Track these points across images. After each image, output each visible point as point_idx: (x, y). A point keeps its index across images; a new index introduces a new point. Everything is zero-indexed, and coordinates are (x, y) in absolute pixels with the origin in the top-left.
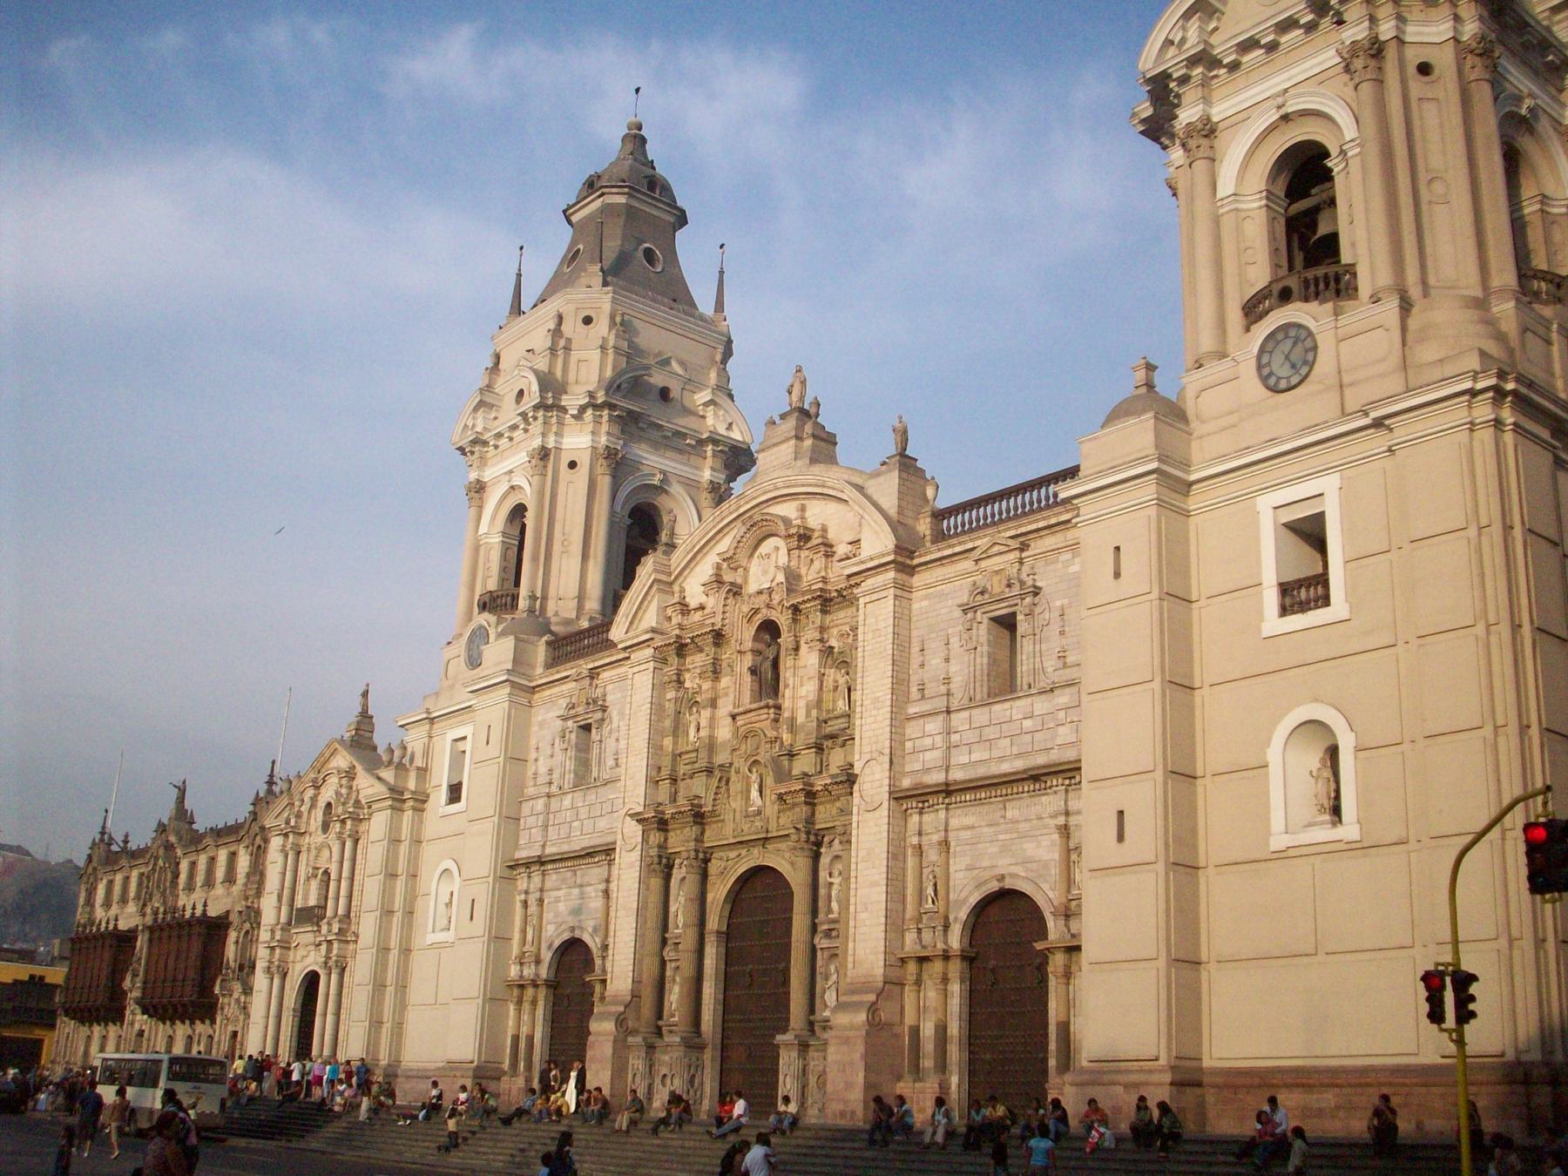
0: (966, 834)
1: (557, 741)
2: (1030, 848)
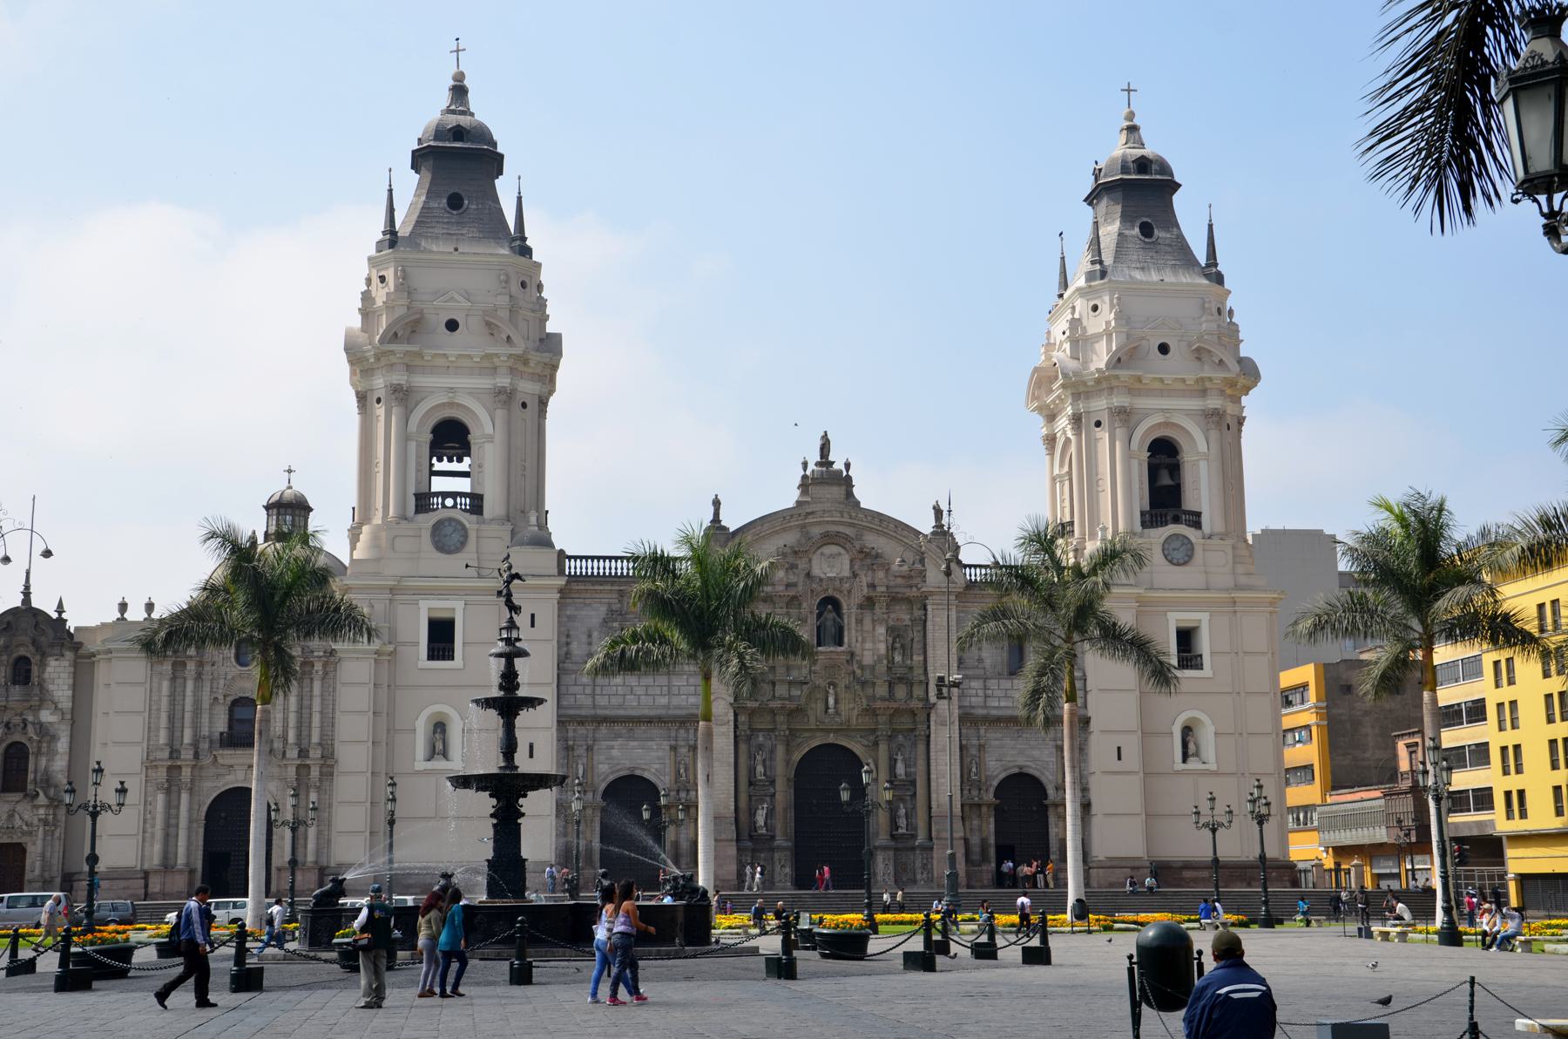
0: (997, 742)
2: (1036, 753)
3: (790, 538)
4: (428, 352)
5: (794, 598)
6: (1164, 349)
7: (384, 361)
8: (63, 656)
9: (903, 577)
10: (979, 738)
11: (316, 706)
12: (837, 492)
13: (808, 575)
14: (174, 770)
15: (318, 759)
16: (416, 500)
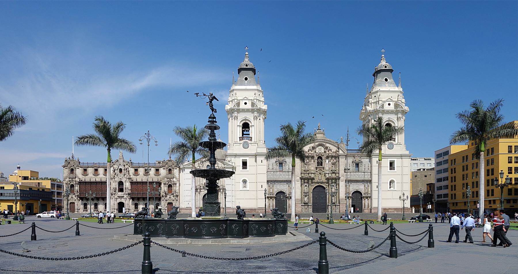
1: (274, 164)
2: (360, 187)
8: (177, 169)
9: (334, 152)
13: (315, 152)
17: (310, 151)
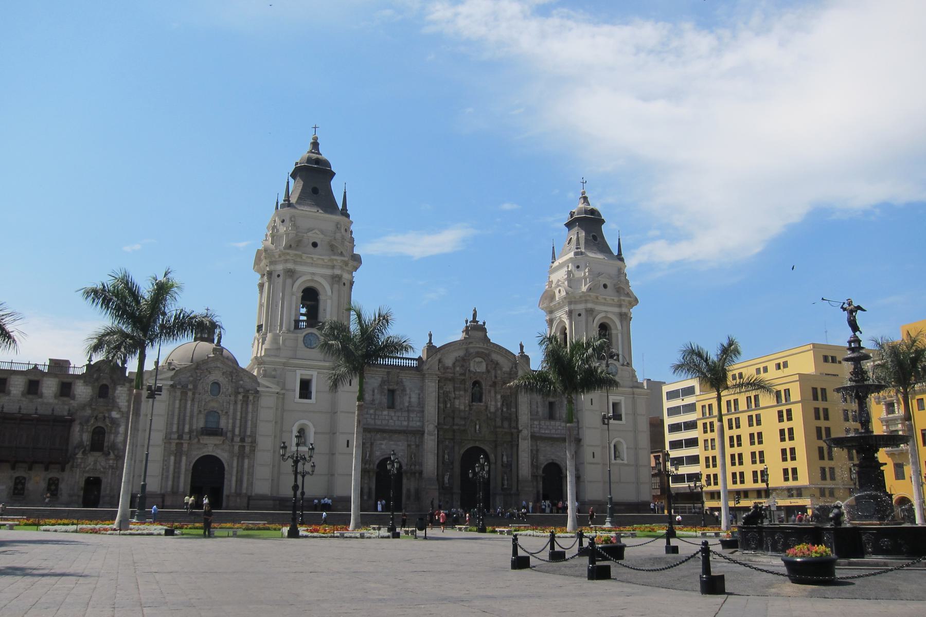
1: (376, 391)
3: (461, 353)
4: (304, 256)
5: (464, 380)
6: (605, 286)
7: (283, 258)
8: (124, 385)
10: (537, 446)
11: (250, 416)
12: (479, 334)
14: (179, 445)
15: (249, 443)
16: (295, 323)
17: (458, 369)
